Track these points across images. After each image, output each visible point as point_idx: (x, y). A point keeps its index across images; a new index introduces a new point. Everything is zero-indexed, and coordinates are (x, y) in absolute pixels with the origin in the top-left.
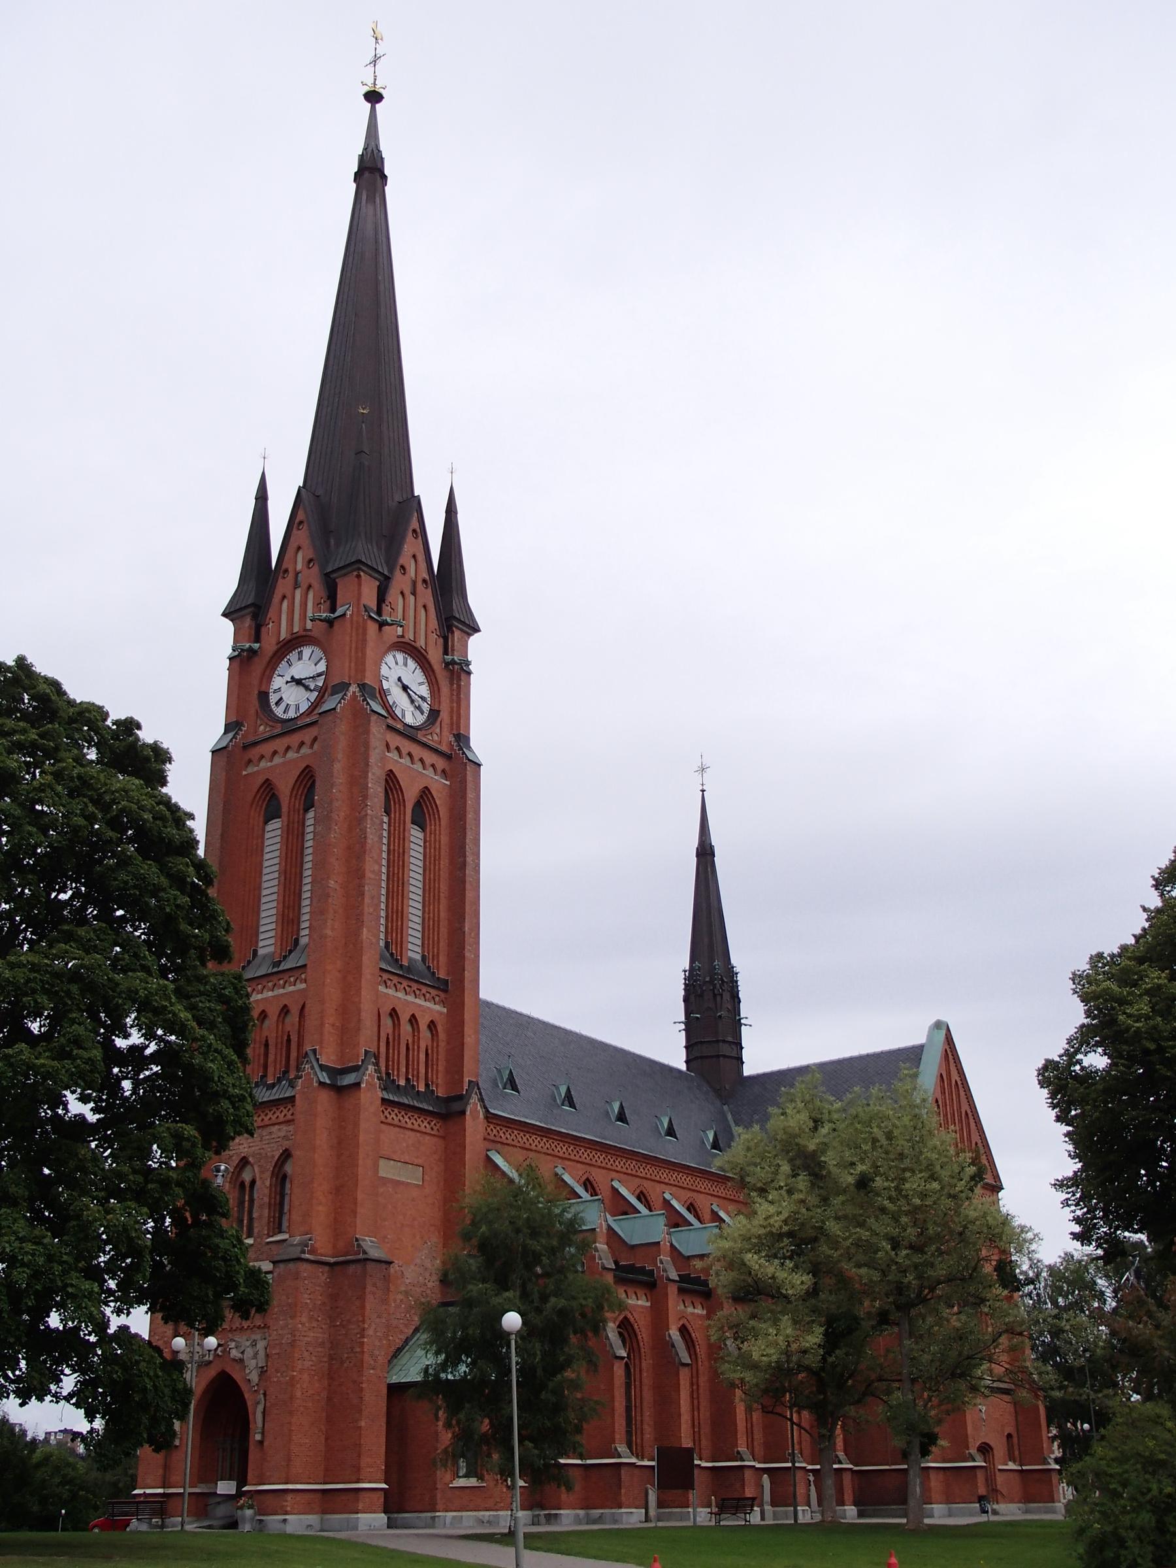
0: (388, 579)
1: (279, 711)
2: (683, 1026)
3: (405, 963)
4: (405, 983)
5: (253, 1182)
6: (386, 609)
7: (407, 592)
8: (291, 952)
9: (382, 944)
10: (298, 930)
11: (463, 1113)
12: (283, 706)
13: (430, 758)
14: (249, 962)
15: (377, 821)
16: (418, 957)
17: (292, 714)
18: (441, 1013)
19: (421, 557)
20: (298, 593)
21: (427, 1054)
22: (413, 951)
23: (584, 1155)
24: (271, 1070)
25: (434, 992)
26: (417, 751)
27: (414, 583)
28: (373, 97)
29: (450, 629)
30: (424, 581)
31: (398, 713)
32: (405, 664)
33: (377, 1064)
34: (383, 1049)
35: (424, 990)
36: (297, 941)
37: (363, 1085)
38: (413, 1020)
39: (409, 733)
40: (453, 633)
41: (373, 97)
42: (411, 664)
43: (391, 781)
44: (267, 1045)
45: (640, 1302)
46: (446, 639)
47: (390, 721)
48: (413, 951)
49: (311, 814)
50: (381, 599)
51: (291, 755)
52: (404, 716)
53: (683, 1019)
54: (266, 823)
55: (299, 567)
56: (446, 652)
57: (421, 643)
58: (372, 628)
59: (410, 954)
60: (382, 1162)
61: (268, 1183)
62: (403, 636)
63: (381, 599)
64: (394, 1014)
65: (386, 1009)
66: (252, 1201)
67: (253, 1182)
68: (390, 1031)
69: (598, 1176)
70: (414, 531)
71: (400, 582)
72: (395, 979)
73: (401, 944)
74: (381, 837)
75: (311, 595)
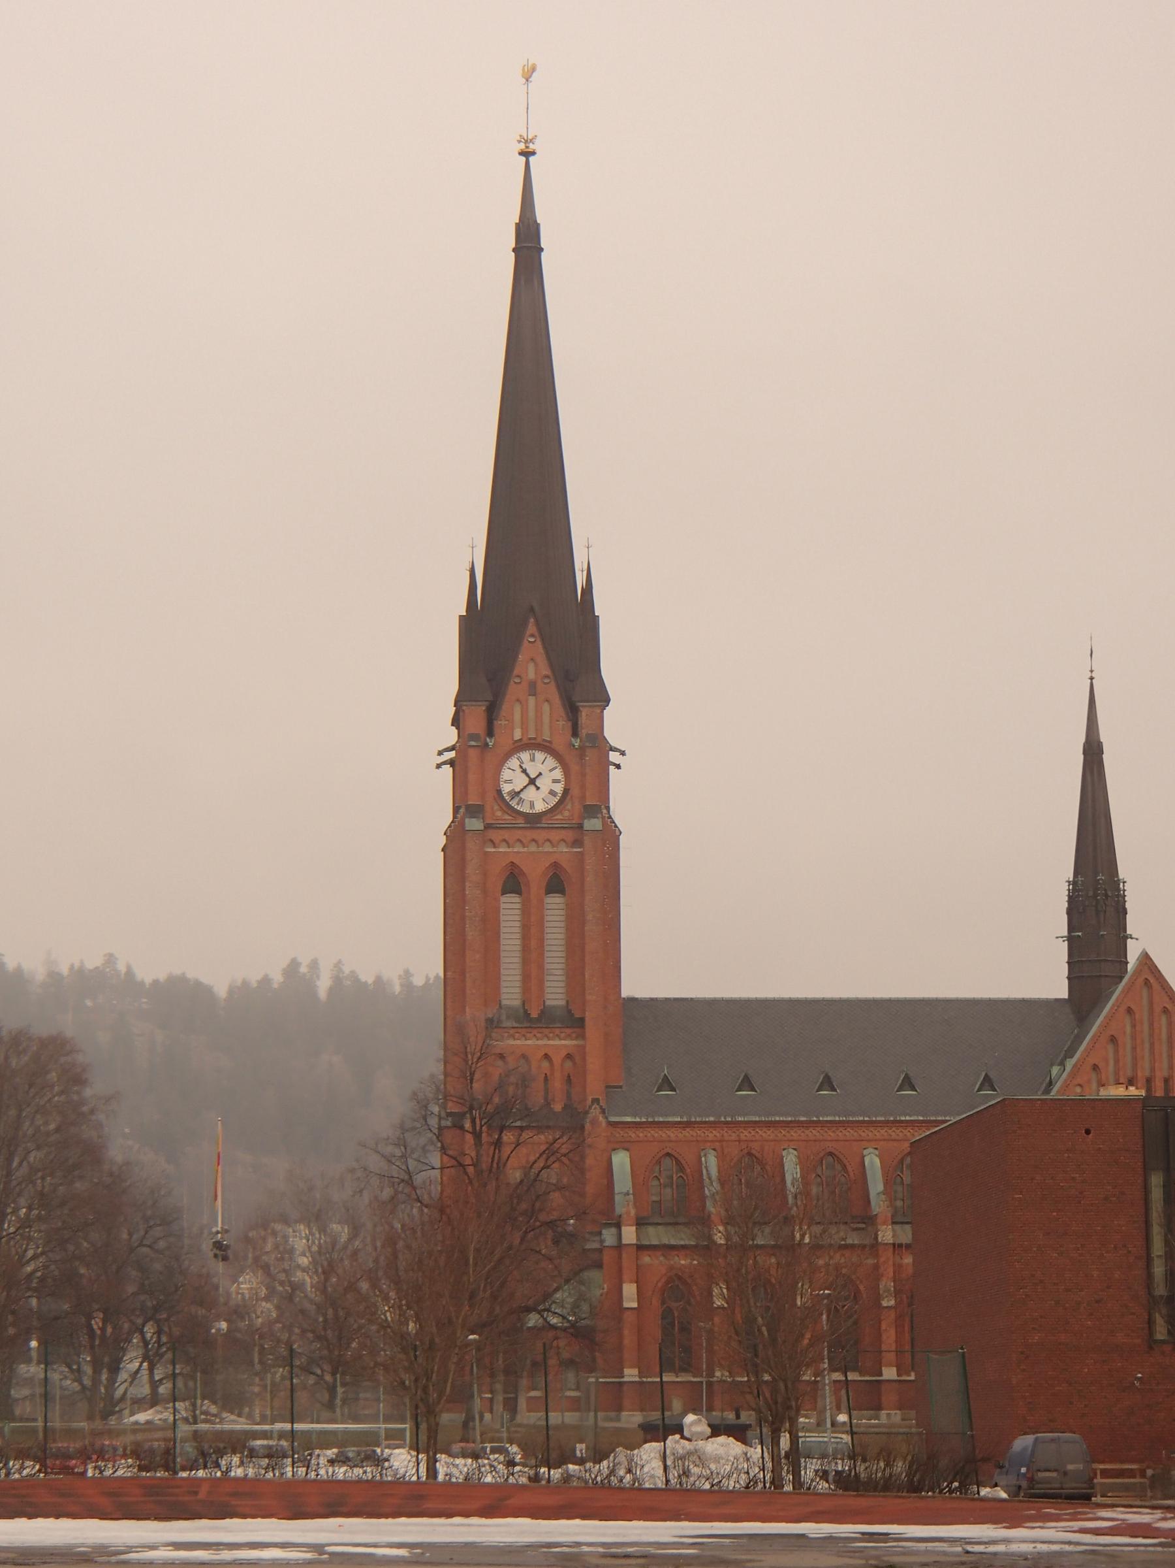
4: (535, 1031)
6: (499, 723)
13: (555, 836)
25: (568, 1031)
26: (540, 835)
28: (527, 154)
35: (557, 1031)
38: (546, 1056)
39: (533, 820)
41: (527, 154)
42: (540, 756)
71: (514, 690)
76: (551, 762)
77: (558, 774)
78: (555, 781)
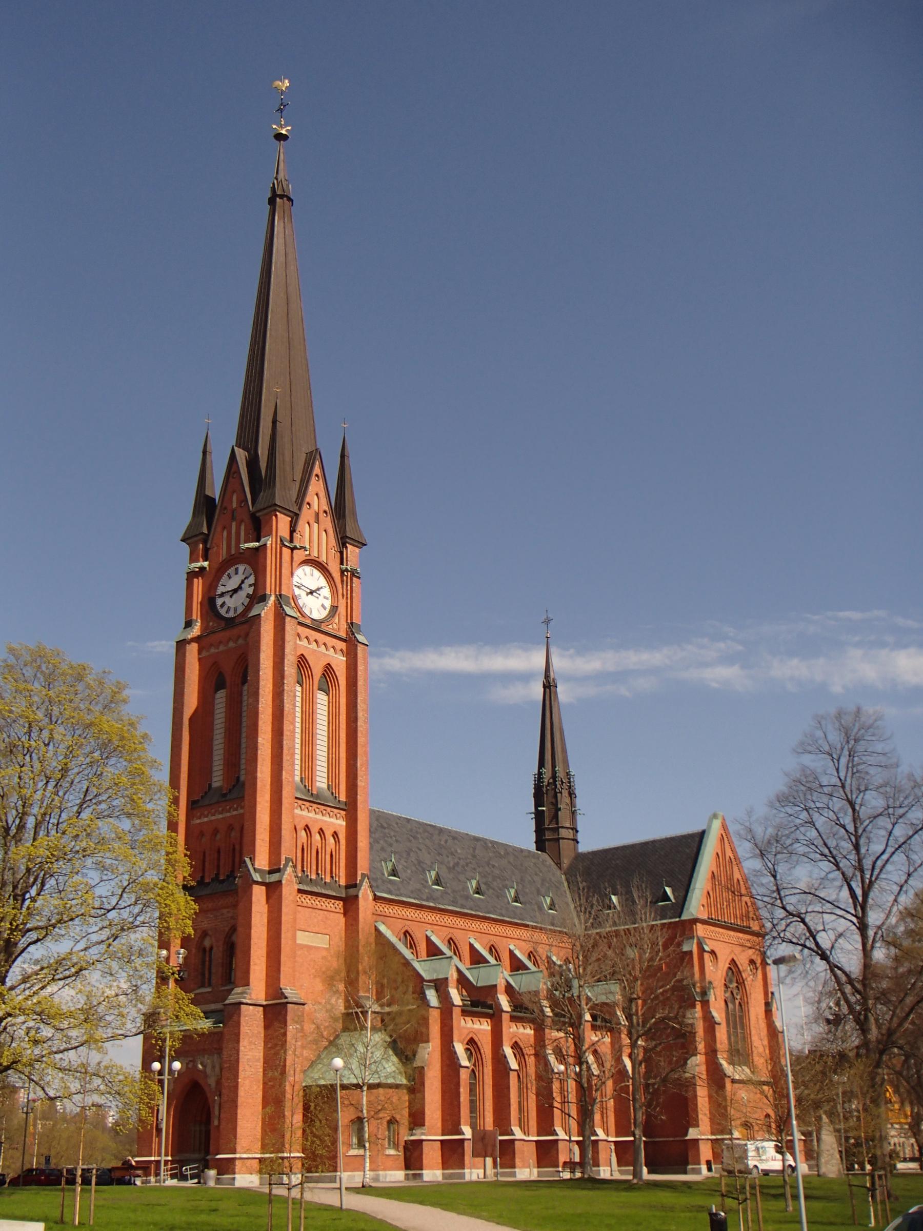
0: (297, 515)
1: (223, 612)
2: (533, 816)
3: (315, 792)
5: (211, 948)
6: (296, 536)
7: (312, 522)
8: (234, 786)
9: (297, 779)
10: (239, 771)
11: (357, 896)
12: (225, 608)
13: (331, 641)
14: (206, 793)
15: (292, 694)
16: (325, 786)
17: (231, 614)
18: (341, 826)
19: (322, 494)
20: (234, 525)
21: (332, 855)
22: (321, 782)
23: (449, 920)
24: (222, 871)
27: (317, 515)
29: (344, 545)
30: (325, 512)
31: (307, 611)
32: (312, 575)
33: (295, 867)
34: (299, 855)
35: (329, 809)
36: (238, 778)
37: (284, 882)
38: (321, 832)
39: (316, 626)
40: (346, 548)
42: (317, 573)
43: (302, 662)
44: (219, 852)
45: (482, 1027)
46: (341, 553)
47: (301, 619)
48: (321, 782)
49: (245, 687)
50: (292, 531)
51: (231, 644)
52: (311, 612)
53: (533, 810)
54: (216, 692)
55: (234, 505)
56: (342, 563)
57: (323, 559)
58: (286, 552)
59: (318, 784)
60: (299, 933)
61: (221, 949)
62: (309, 555)
63: (292, 531)
64: (307, 828)
65: (302, 825)
66: (210, 961)
67: (211, 948)
68: (305, 841)
69: (458, 936)
70: (317, 475)
71: (306, 514)
72: (308, 804)
73: (312, 780)
74: (294, 705)
75: (243, 527)
76: (322, 582)
77: (326, 592)
78: (325, 598)
